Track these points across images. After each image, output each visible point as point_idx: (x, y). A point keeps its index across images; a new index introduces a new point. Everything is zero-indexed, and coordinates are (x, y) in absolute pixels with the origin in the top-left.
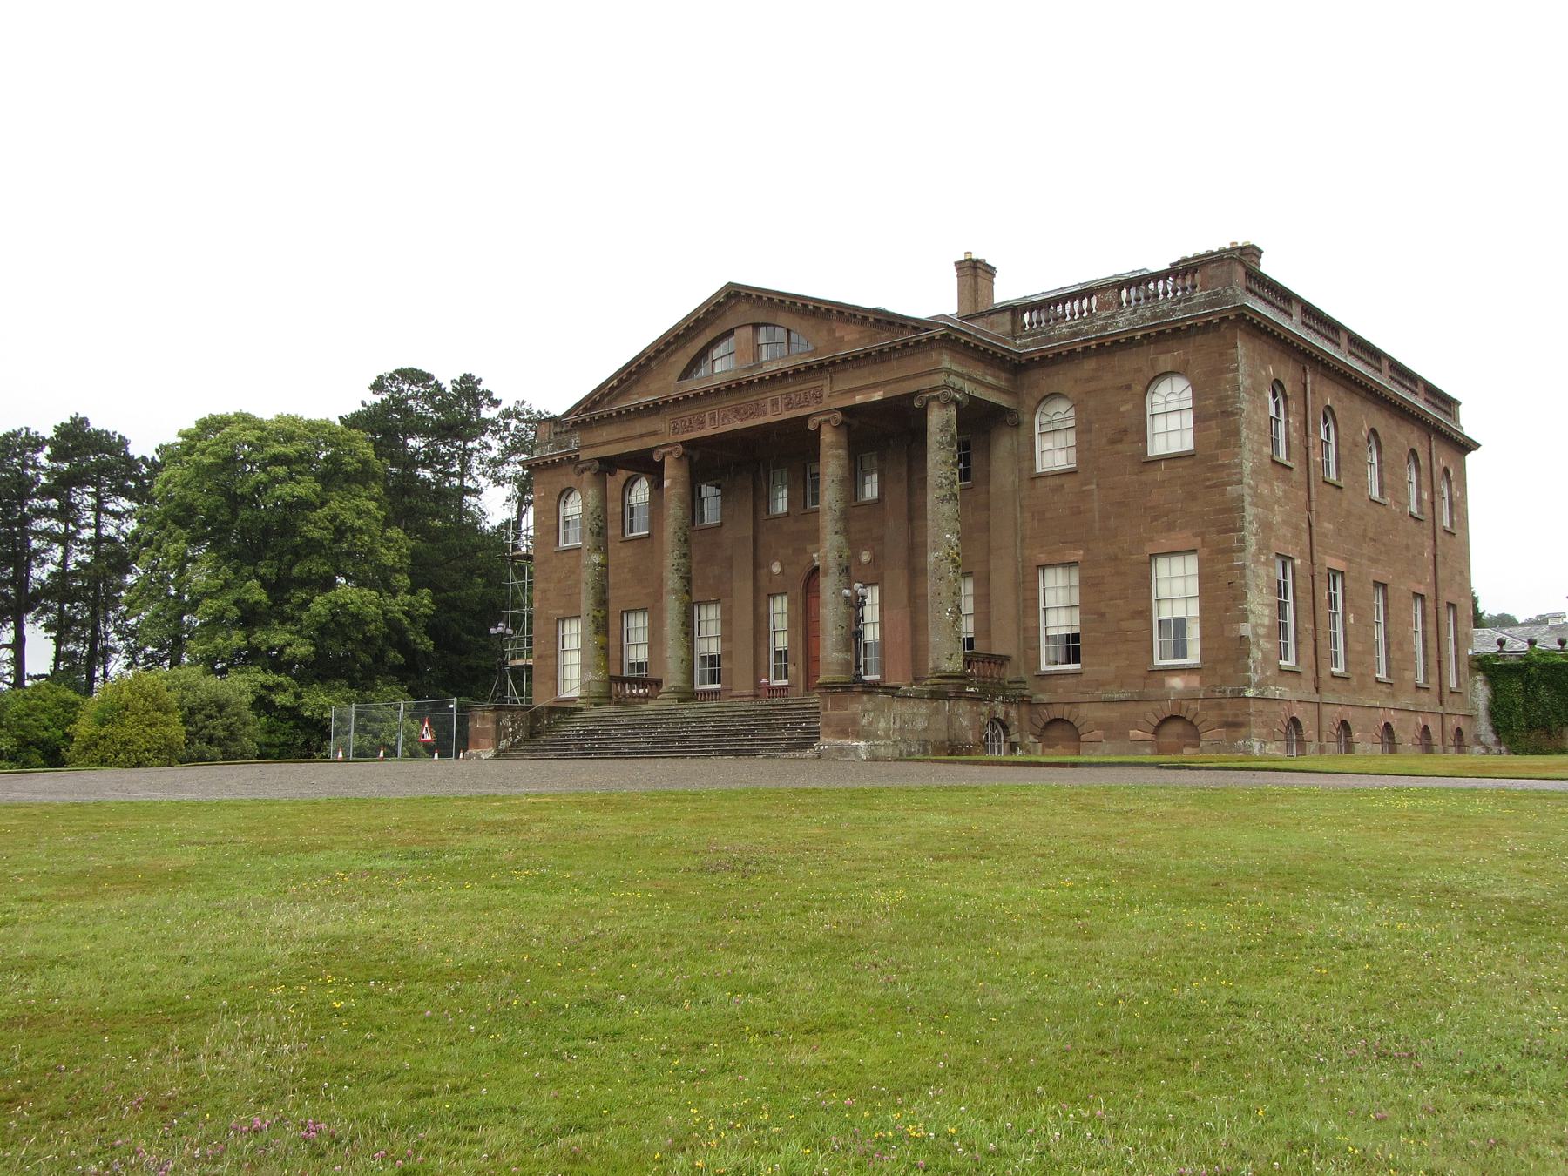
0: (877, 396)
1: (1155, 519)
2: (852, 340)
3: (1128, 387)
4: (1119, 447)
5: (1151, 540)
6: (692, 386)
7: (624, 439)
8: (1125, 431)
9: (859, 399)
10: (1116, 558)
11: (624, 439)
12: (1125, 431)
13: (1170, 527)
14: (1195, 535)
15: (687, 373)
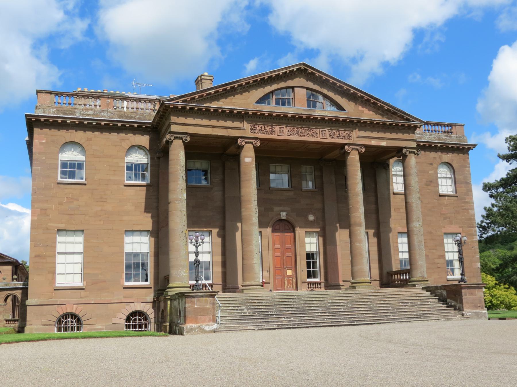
0: (383, 144)
1: (445, 219)
2: (367, 114)
3: (432, 164)
4: (429, 187)
5: (444, 227)
6: (265, 108)
7: (213, 127)
8: (431, 182)
9: (373, 143)
10: (431, 233)
11: (213, 127)
12: (431, 182)
13: (451, 223)
14: (460, 227)
15: (263, 100)
